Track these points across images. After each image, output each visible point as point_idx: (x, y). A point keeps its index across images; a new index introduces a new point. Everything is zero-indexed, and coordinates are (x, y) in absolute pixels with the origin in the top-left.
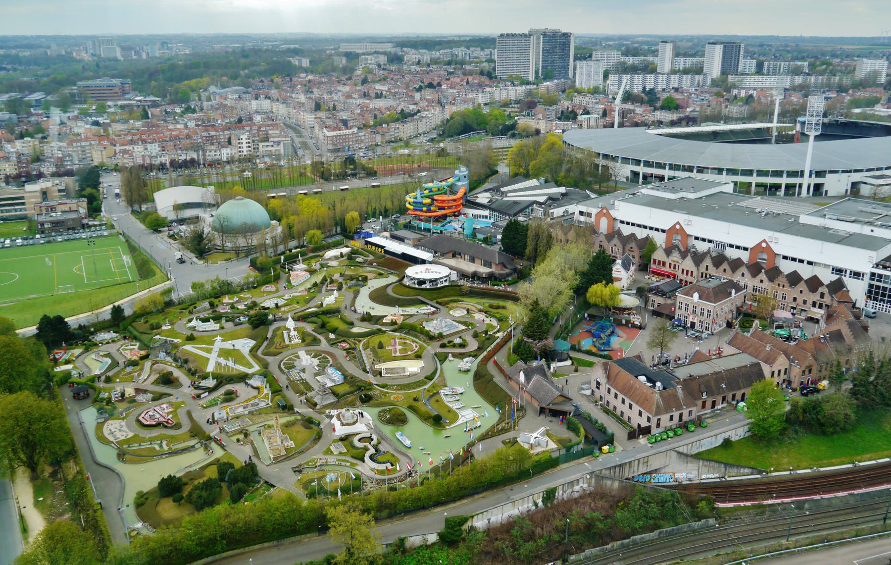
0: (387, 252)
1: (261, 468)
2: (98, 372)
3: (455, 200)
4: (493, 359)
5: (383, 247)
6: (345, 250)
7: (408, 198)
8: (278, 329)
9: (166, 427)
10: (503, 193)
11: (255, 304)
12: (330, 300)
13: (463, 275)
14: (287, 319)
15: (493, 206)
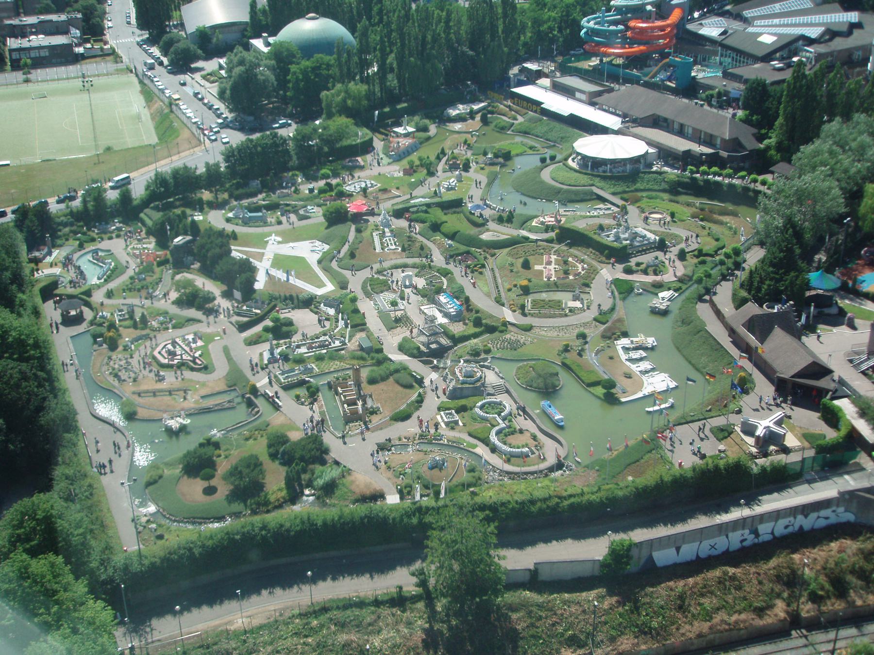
2: (95, 281)
3: (662, 29)
7: (584, 22)
9: (193, 369)
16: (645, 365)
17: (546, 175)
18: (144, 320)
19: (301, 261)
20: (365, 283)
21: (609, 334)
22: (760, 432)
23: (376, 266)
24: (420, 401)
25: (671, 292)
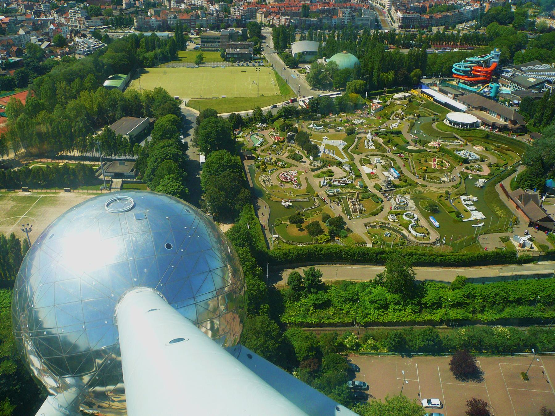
0: (435, 100)
1: (346, 219)
4: (500, 183)
5: (432, 97)
6: (407, 94)
7: (454, 66)
8: (360, 138)
10: (523, 71)
11: (348, 121)
12: (394, 125)
13: (485, 123)
14: (368, 133)
15: (514, 79)
16: (473, 208)
17: (434, 125)
18: (276, 163)
19: (336, 147)
20: (361, 159)
21: (458, 193)
22: (522, 242)
23: (366, 154)
24: (382, 209)
25: (484, 179)
